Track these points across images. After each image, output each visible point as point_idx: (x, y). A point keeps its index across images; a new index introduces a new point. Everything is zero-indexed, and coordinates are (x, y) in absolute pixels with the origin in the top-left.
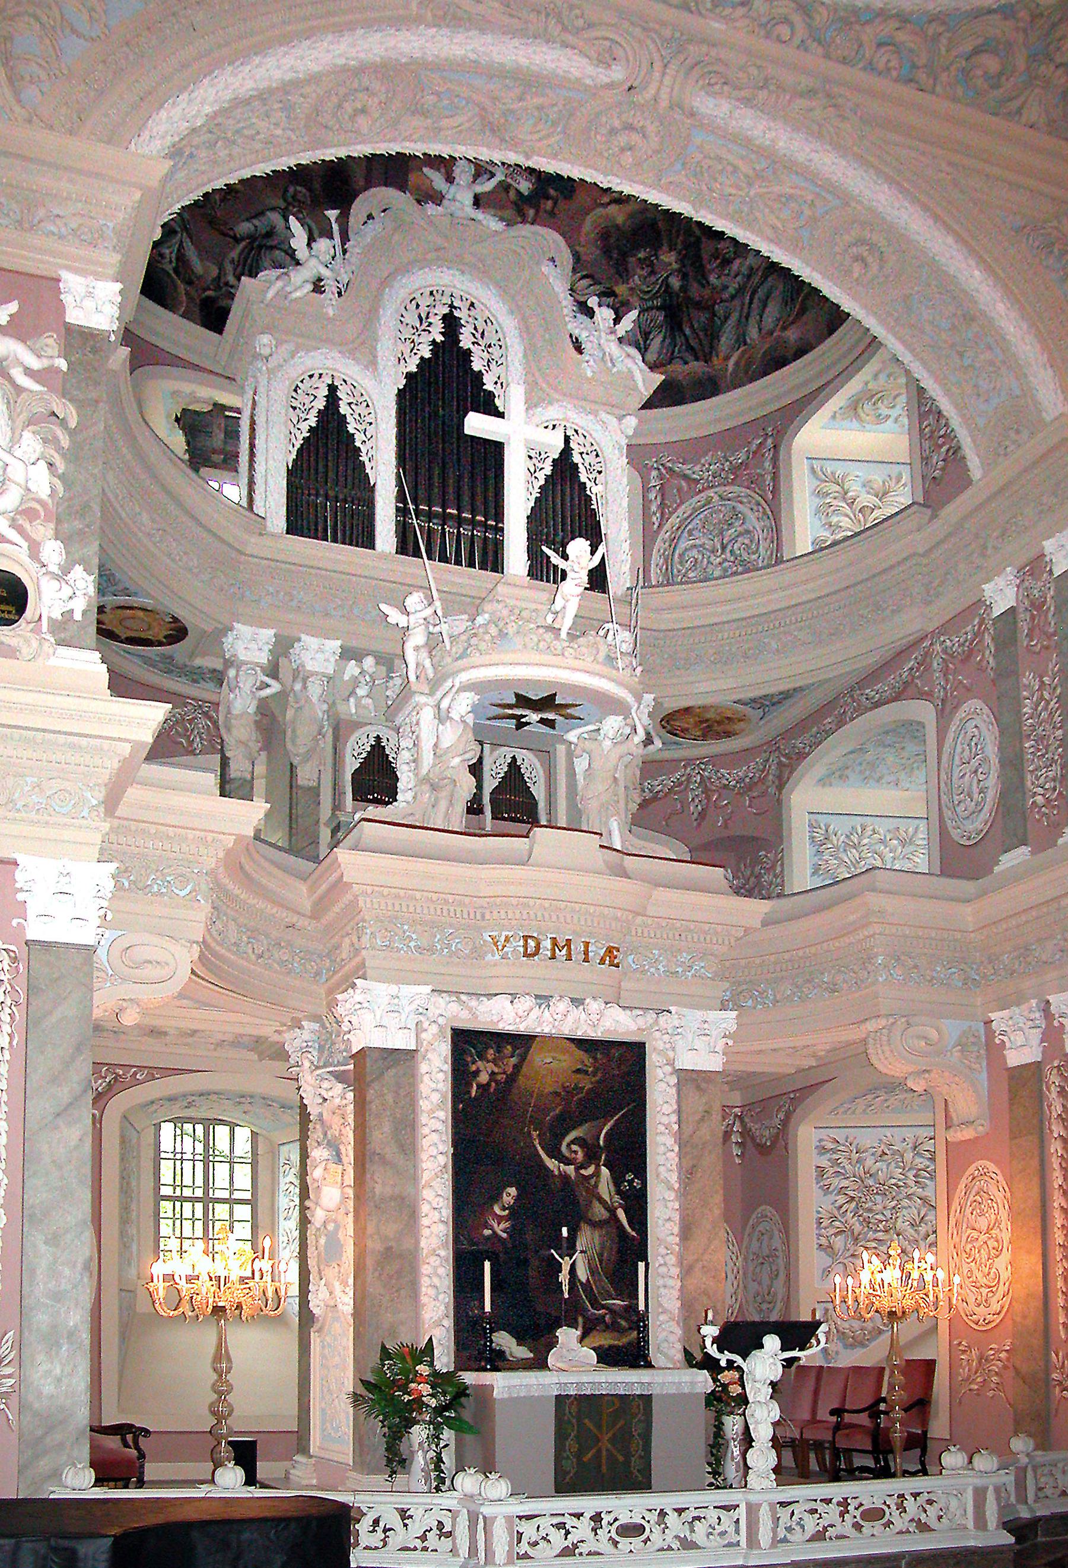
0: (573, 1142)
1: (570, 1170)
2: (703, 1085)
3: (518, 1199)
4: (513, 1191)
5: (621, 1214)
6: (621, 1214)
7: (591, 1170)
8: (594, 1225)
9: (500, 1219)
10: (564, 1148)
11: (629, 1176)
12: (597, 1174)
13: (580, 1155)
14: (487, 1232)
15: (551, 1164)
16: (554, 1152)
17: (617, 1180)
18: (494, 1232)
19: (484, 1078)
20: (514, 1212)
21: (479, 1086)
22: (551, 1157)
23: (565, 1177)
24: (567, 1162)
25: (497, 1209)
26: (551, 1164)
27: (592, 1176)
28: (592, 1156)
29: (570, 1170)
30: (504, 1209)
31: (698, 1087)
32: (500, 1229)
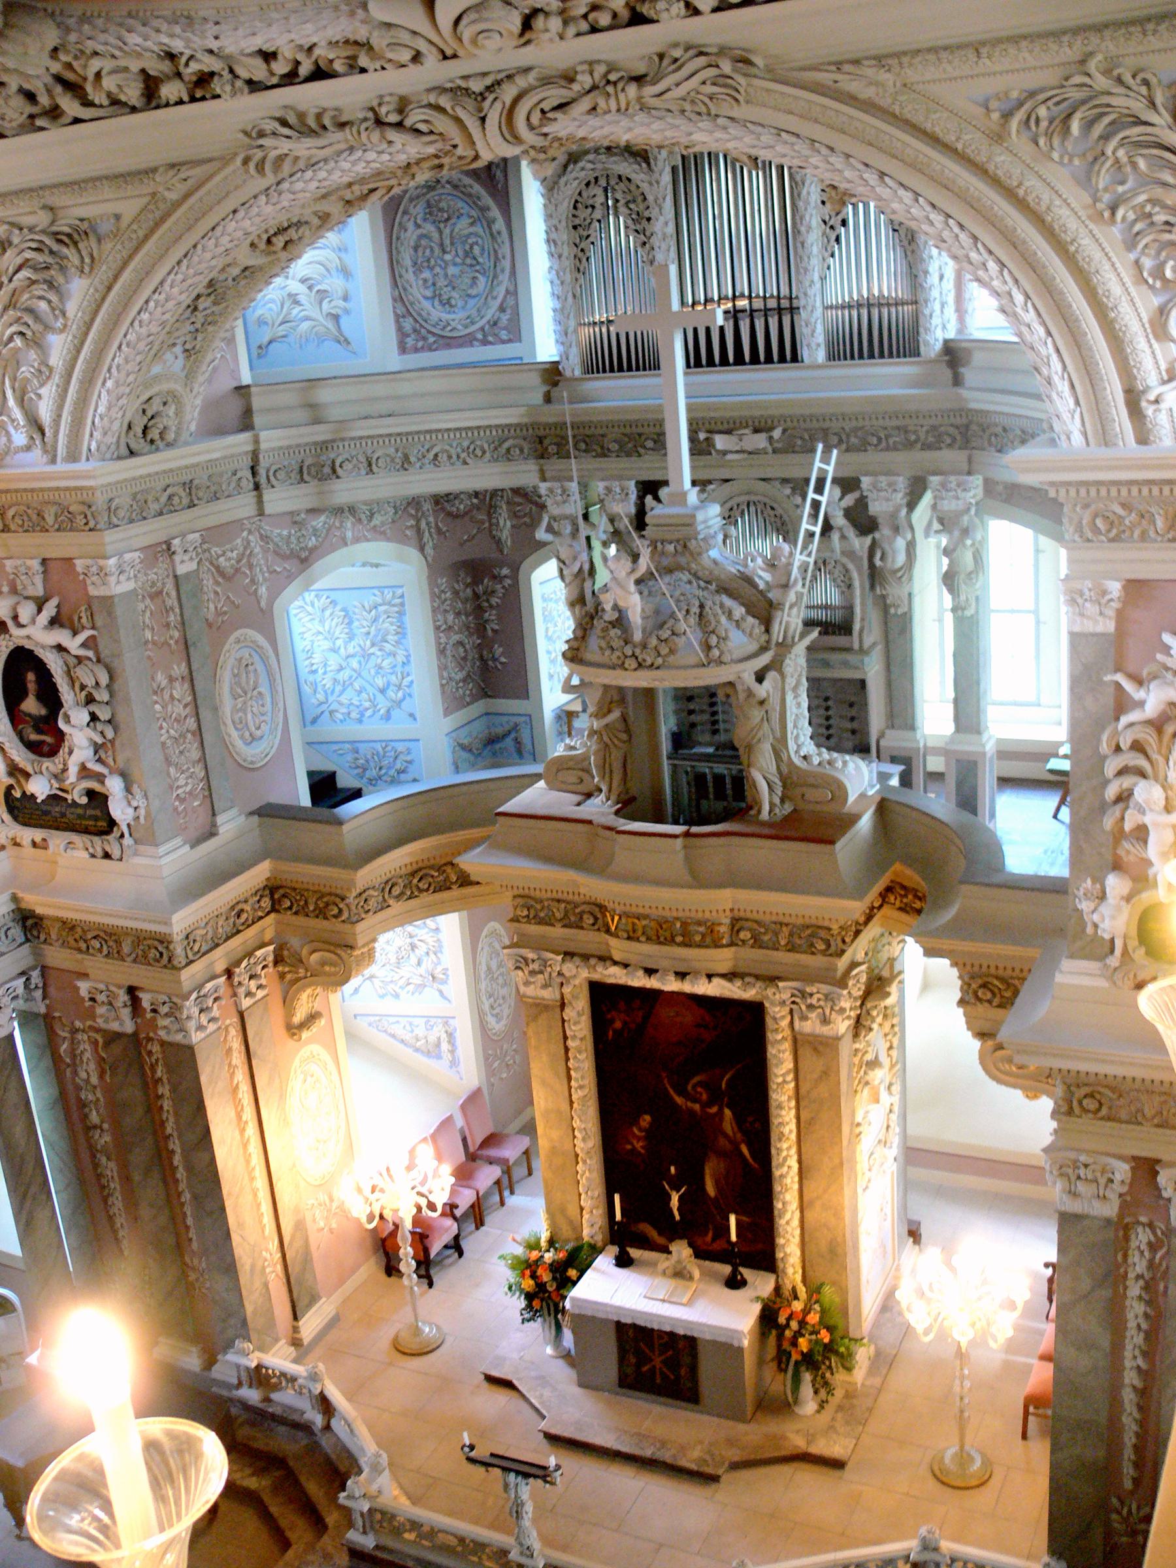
0: (699, 1084)
1: (697, 1107)
2: (821, 1048)
3: (651, 1124)
4: (648, 1118)
5: (745, 1150)
6: (745, 1150)
7: (714, 1110)
8: (722, 1154)
9: (639, 1139)
10: (689, 1088)
11: (750, 1119)
12: (720, 1113)
13: (704, 1096)
14: (629, 1147)
15: (679, 1100)
16: (682, 1092)
17: (739, 1119)
18: (634, 1148)
19: (618, 1025)
20: (650, 1134)
21: (615, 1031)
22: (679, 1095)
23: (691, 1112)
24: (695, 1101)
25: (635, 1130)
26: (679, 1100)
27: (715, 1114)
28: (715, 1097)
29: (697, 1107)
30: (640, 1130)
31: (815, 1049)
32: (639, 1145)
